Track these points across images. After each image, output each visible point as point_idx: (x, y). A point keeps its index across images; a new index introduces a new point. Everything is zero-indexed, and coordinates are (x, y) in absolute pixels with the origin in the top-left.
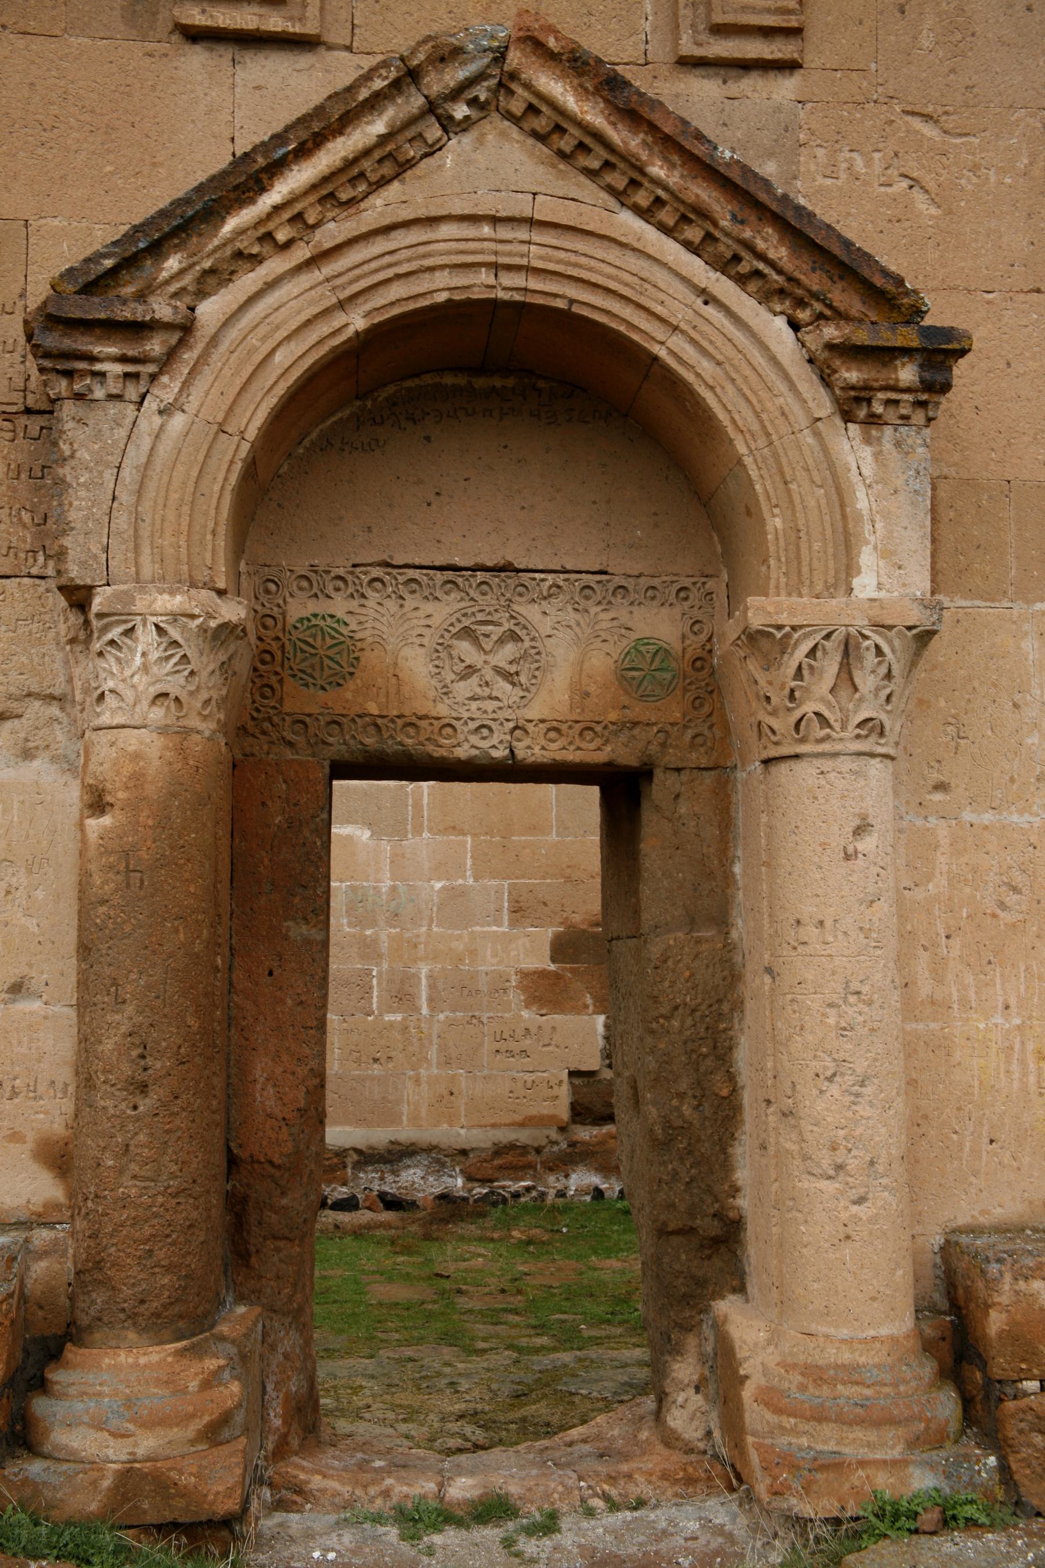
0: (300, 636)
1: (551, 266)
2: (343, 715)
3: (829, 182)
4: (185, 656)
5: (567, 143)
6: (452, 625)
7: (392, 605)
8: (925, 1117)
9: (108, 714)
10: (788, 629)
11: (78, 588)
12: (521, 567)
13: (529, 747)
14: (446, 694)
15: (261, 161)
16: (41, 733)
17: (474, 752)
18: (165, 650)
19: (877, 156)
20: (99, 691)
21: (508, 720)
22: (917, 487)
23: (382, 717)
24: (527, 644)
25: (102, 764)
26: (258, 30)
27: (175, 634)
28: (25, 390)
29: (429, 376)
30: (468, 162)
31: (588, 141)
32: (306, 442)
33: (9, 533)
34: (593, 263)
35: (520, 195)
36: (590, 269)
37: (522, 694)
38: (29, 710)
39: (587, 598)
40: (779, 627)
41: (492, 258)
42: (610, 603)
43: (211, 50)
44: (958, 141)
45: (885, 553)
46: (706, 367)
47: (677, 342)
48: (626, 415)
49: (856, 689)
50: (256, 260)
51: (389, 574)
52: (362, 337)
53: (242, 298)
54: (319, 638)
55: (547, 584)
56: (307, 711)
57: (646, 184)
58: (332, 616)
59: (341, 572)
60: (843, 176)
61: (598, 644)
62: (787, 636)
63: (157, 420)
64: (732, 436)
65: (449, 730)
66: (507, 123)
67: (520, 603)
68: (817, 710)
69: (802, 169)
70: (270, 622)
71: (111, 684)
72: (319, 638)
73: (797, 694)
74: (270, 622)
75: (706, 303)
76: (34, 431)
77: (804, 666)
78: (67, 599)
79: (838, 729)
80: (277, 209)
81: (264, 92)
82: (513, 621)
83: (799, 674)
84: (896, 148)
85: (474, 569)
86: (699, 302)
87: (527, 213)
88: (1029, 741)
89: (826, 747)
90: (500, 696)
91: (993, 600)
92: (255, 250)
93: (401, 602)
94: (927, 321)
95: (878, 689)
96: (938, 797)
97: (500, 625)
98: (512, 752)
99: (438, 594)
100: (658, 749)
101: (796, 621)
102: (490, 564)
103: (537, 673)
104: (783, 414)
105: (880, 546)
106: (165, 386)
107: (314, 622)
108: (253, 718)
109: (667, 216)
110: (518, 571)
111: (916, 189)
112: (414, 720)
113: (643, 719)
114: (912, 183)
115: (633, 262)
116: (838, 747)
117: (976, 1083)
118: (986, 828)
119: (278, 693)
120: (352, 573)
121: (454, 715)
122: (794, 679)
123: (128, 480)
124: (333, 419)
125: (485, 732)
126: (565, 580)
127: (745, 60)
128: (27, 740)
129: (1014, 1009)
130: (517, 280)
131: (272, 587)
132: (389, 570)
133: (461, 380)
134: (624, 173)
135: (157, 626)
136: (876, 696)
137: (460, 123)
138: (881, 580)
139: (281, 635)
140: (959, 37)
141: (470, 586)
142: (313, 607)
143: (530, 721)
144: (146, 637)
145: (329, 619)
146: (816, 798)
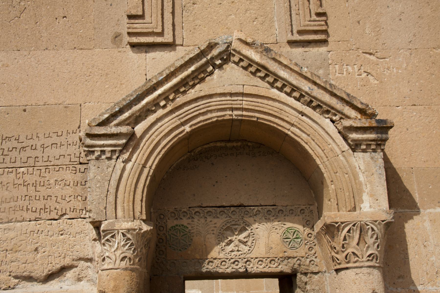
1: (250, 107)
3: (340, 75)
4: (132, 243)
5: (253, 69)
6: (223, 226)
7: (203, 220)
9: (106, 265)
10: (339, 223)
11: (96, 222)
12: (246, 205)
13: (252, 268)
14: (222, 250)
15: (155, 81)
16: (84, 272)
17: (234, 270)
18: (126, 242)
19: (355, 66)
20: (103, 257)
21: (245, 258)
22: (380, 172)
23: (201, 259)
24: (250, 231)
25: (104, 283)
26: (153, 42)
27: (129, 236)
28: (80, 157)
29: (212, 144)
30: (221, 77)
31: (259, 68)
32: (172, 168)
33: (74, 204)
34: (264, 105)
35: (239, 86)
36: (263, 107)
37: (249, 249)
38: (80, 264)
39: (269, 214)
40: (337, 223)
41: (231, 106)
42: (277, 216)
43: (139, 49)
44: (382, 60)
45: (371, 195)
46: (304, 136)
47: (293, 129)
48: (279, 153)
49: (366, 243)
50: (155, 112)
51: (201, 210)
52: (189, 133)
53: (149, 124)
54: (178, 233)
55: (255, 210)
57: (280, 80)
58: (183, 225)
59: (185, 210)
60: (345, 73)
61: (274, 230)
62: (339, 226)
63: (122, 165)
64: (315, 158)
65: (224, 263)
66: (233, 64)
67: (246, 218)
69: (331, 72)
70: (162, 229)
71: (107, 254)
72: (178, 233)
73: (345, 246)
74: (162, 229)
75: (302, 116)
76: (82, 170)
78: (93, 225)
79: (361, 258)
80: (160, 95)
81: (155, 60)
82: (244, 224)
83: (345, 239)
84: (362, 64)
85: (230, 207)
86: (300, 115)
87: (242, 91)
88: (432, 259)
89: (357, 264)
90: (241, 250)
91: (412, 209)
92: (154, 108)
93: (206, 219)
94: (378, 118)
95: (374, 243)
96: (400, 280)
97: (240, 225)
99: (218, 216)
100: (297, 266)
101: (343, 220)
102: (235, 205)
103: (253, 241)
104: (331, 150)
105: (369, 193)
106: (124, 153)
108: (156, 262)
109: (287, 89)
110: (245, 206)
111: (369, 76)
113: (291, 255)
114: (368, 74)
115: (277, 104)
116: (362, 264)
120: (189, 210)
121: (226, 257)
122: (344, 241)
123: (113, 185)
124: (181, 159)
125: (236, 263)
126: (261, 209)
127: (309, 40)
128: (79, 275)
130: (240, 113)
131: (162, 216)
132: (201, 208)
133: (223, 144)
134: (272, 77)
135: (122, 233)
136: (374, 245)
137: (218, 65)
138: (371, 204)
140: (379, 29)
141: (229, 212)
142: (176, 222)
143: (252, 258)
144: (119, 237)
145: (181, 226)
146: (355, 283)
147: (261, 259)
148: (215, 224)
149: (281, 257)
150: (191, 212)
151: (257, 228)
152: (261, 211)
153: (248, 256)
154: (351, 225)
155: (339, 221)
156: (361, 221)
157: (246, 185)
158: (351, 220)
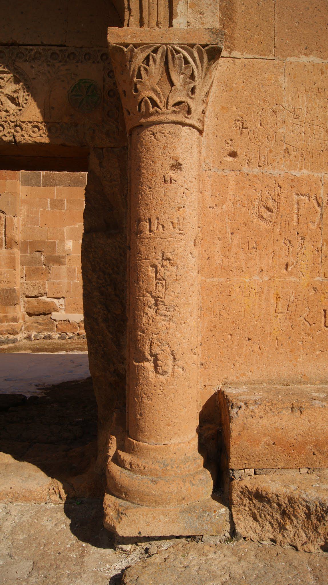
8: (215, 327)
10: (131, 45)
12: (21, 43)
40: (127, 45)
68: (149, 95)
73: (138, 86)
77: (142, 69)
91: (264, 55)
101: (135, 41)
102: (5, 42)
116: (162, 118)
117: (243, 310)
118: (255, 176)
126: (43, 50)
129: (265, 272)
138: (189, 20)
143: (23, 122)
147: (36, 124)
149: (65, 123)
152: (43, 53)
153: (18, 118)
154: (149, 51)
155: (129, 42)
156: (166, 44)
157: (22, 13)
158: (150, 42)
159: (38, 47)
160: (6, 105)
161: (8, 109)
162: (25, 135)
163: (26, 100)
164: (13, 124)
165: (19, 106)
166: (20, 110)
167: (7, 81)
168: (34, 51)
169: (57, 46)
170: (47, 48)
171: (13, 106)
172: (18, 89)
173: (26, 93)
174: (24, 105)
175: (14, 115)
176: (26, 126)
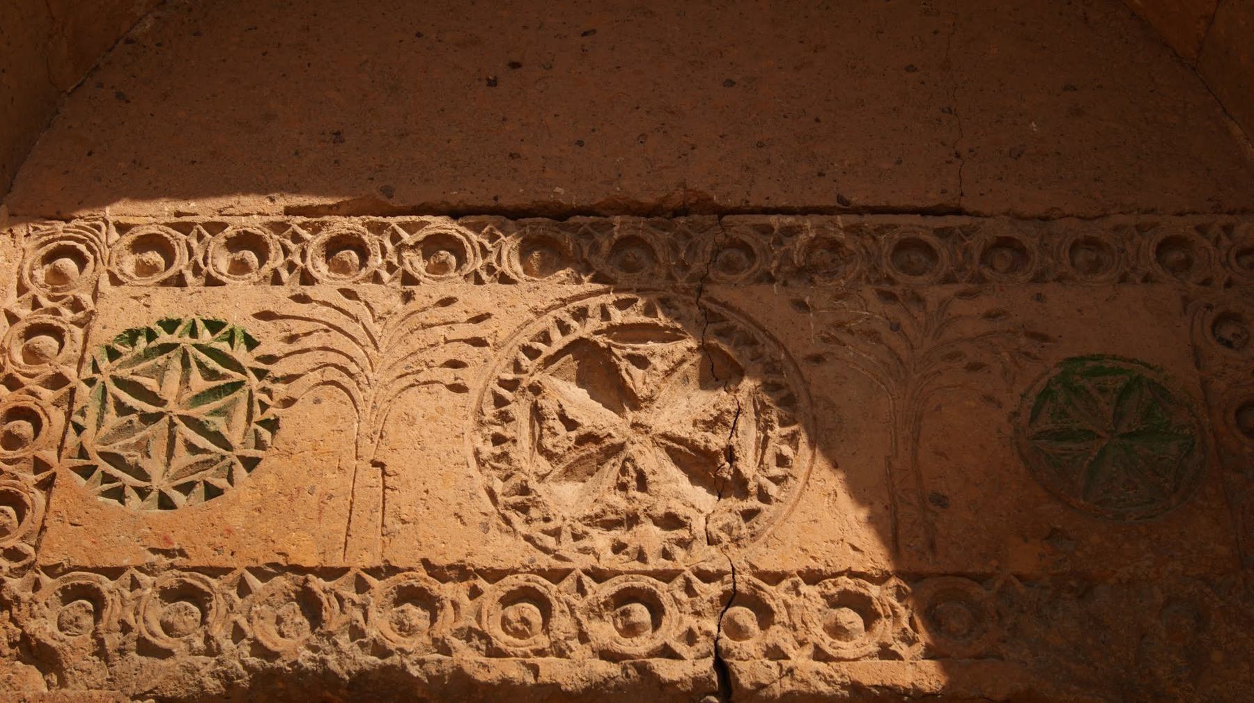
0: (125, 373)
2: (215, 572)
12: (731, 202)
17: (603, 668)
42: (980, 279)
51: (378, 229)
54: (174, 375)
56: (109, 560)
58: (214, 326)
74: (46, 342)
98: (721, 666)
102: (648, 199)
107: (164, 337)
110: (721, 212)
112: (420, 578)
119: (34, 517)
120: (279, 228)
121: (545, 561)
126: (849, 229)
131: (68, 264)
139: (70, 372)
141: (595, 248)
143: (775, 578)
145: (205, 336)
148: (478, 319)
150: (296, 238)
151: (818, 359)
152: (850, 246)
153: (739, 557)
159: (824, 219)
160: (664, 489)
161: (679, 509)
162: (788, 646)
163: (782, 461)
164: (715, 589)
165: (743, 493)
166: (749, 515)
167: (668, 373)
168: (802, 236)
169: (923, 212)
170: (869, 220)
171: (702, 497)
172: (733, 408)
173: (777, 428)
174: (773, 489)
175: (711, 541)
176: (792, 599)
